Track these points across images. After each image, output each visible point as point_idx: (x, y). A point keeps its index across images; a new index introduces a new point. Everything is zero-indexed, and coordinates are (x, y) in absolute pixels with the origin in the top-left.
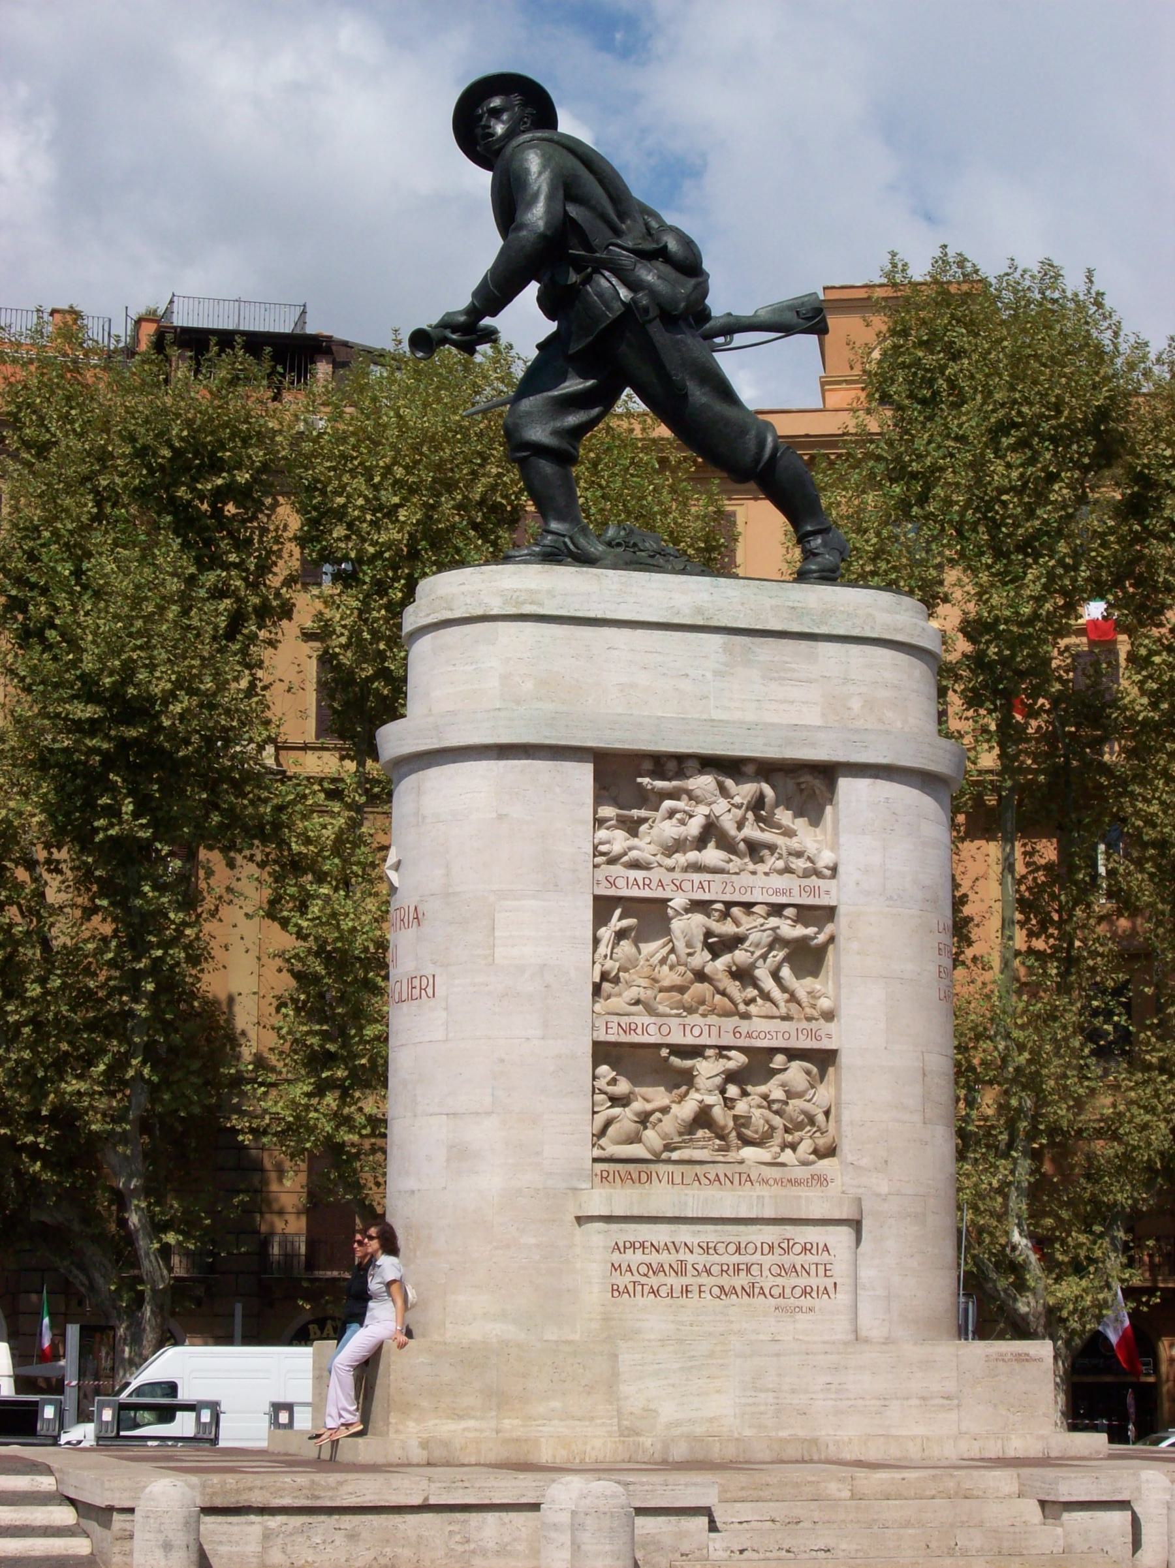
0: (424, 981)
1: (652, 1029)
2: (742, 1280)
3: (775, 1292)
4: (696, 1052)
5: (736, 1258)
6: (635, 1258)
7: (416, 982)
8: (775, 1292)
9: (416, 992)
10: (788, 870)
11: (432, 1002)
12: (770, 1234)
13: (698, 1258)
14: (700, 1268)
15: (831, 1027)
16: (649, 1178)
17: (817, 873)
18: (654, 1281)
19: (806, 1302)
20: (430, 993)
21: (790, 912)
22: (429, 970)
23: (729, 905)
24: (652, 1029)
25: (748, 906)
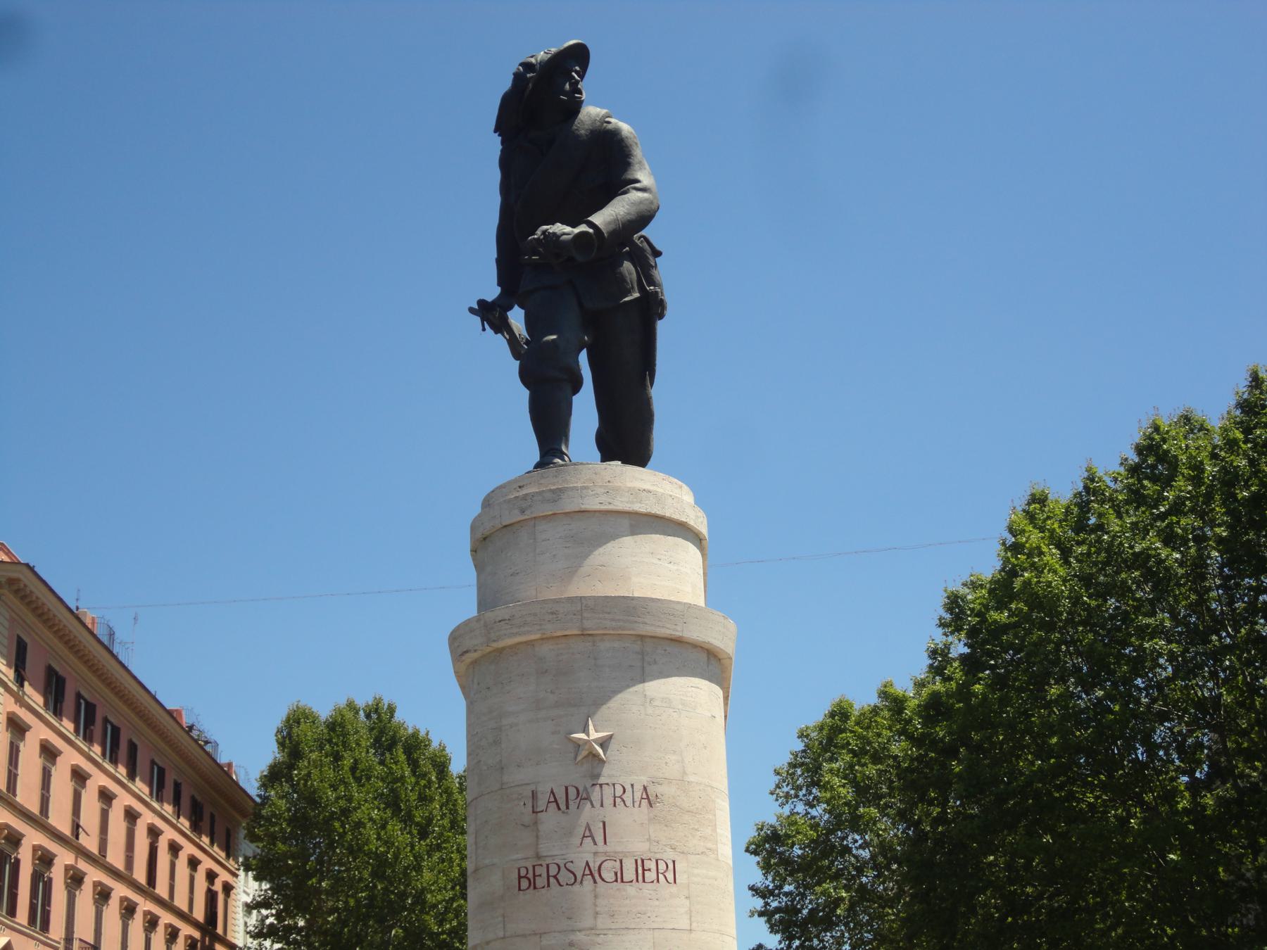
0: (662, 866)
7: (648, 864)
9: (650, 876)
11: (673, 889)
20: (670, 876)
22: (669, 855)
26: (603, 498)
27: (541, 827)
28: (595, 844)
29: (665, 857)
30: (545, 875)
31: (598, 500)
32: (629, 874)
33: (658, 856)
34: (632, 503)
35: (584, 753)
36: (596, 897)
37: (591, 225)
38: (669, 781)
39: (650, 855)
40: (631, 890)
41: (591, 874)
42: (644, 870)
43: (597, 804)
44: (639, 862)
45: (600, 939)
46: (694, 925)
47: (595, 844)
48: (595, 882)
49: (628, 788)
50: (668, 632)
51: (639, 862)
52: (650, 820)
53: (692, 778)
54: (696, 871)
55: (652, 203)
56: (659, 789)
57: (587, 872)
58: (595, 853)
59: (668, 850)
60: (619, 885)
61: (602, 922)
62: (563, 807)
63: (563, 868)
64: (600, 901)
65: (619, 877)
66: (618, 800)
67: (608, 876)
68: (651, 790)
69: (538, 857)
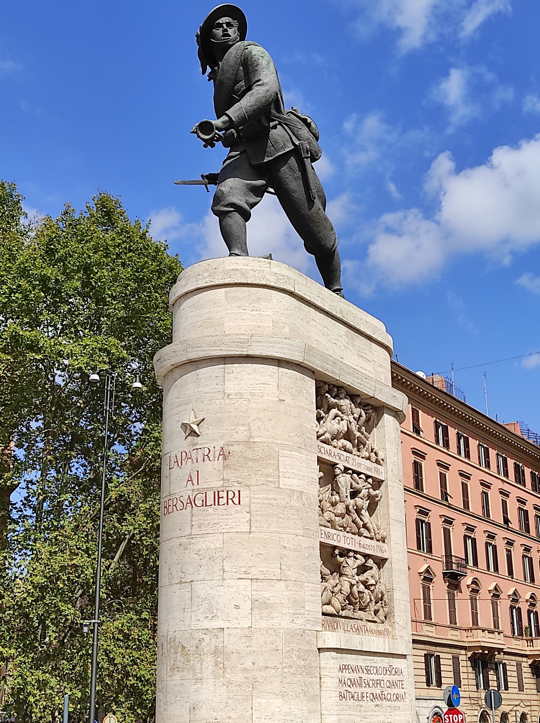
0: (231, 495)
1: (335, 537)
2: (377, 691)
3: (389, 697)
4: (345, 553)
5: (376, 677)
6: (346, 675)
8: (389, 697)
9: (223, 501)
10: (369, 459)
11: (238, 508)
12: (385, 662)
13: (364, 676)
14: (366, 681)
15: (385, 546)
16: (337, 626)
17: (377, 462)
18: (352, 690)
19: (397, 704)
20: (236, 500)
21: (370, 480)
23: (354, 472)
24: (335, 537)
25: (359, 474)
26: (208, 279)
27: (172, 477)
28: (193, 485)
29: (232, 489)
30: (172, 505)
31: (205, 281)
32: (210, 501)
33: (228, 489)
34: (225, 279)
35: (188, 432)
36: (192, 516)
37: (228, 116)
38: (239, 443)
39: (223, 489)
40: (211, 510)
41: (191, 503)
42: (219, 498)
43: (195, 461)
44: (216, 493)
45: (193, 541)
46: (253, 529)
47: (193, 485)
48: (192, 507)
49: (212, 449)
50: (237, 353)
51: (216, 493)
52: (224, 467)
53: (256, 440)
54: (256, 496)
55: (268, 91)
56: (231, 448)
57: (189, 502)
58: (193, 490)
59: (236, 484)
60: (204, 507)
61: (196, 530)
62: (180, 465)
63: (178, 500)
64: (194, 518)
65: (205, 504)
66: (206, 457)
67: (199, 503)
68: (226, 449)
69: (170, 495)
